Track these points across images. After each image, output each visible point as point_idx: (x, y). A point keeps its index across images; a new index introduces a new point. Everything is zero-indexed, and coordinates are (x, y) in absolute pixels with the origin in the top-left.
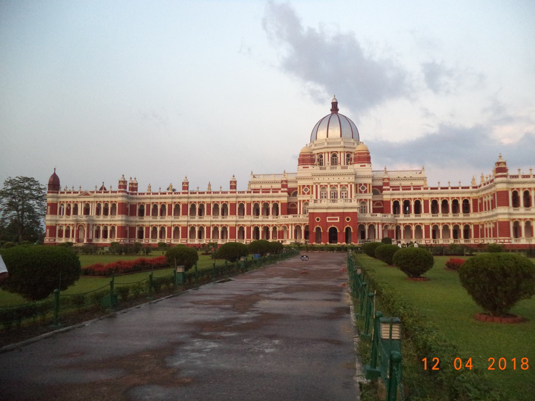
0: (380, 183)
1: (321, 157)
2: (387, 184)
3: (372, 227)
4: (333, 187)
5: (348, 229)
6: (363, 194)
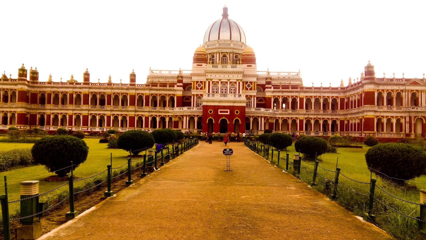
0: (263, 82)
1: (213, 57)
2: (269, 83)
3: (256, 120)
4: (224, 83)
6: (249, 91)
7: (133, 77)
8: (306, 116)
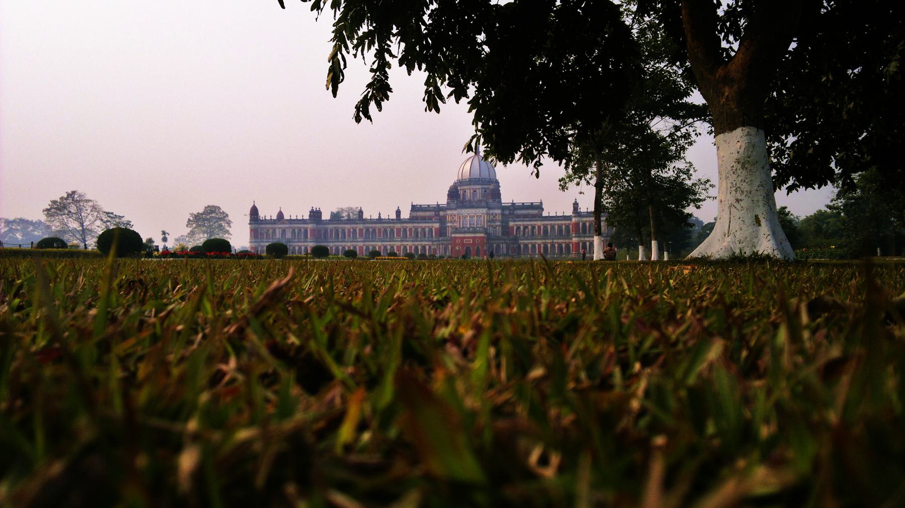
1: (465, 192)
5: (478, 247)
7: (398, 213)
8: (544, 241)
